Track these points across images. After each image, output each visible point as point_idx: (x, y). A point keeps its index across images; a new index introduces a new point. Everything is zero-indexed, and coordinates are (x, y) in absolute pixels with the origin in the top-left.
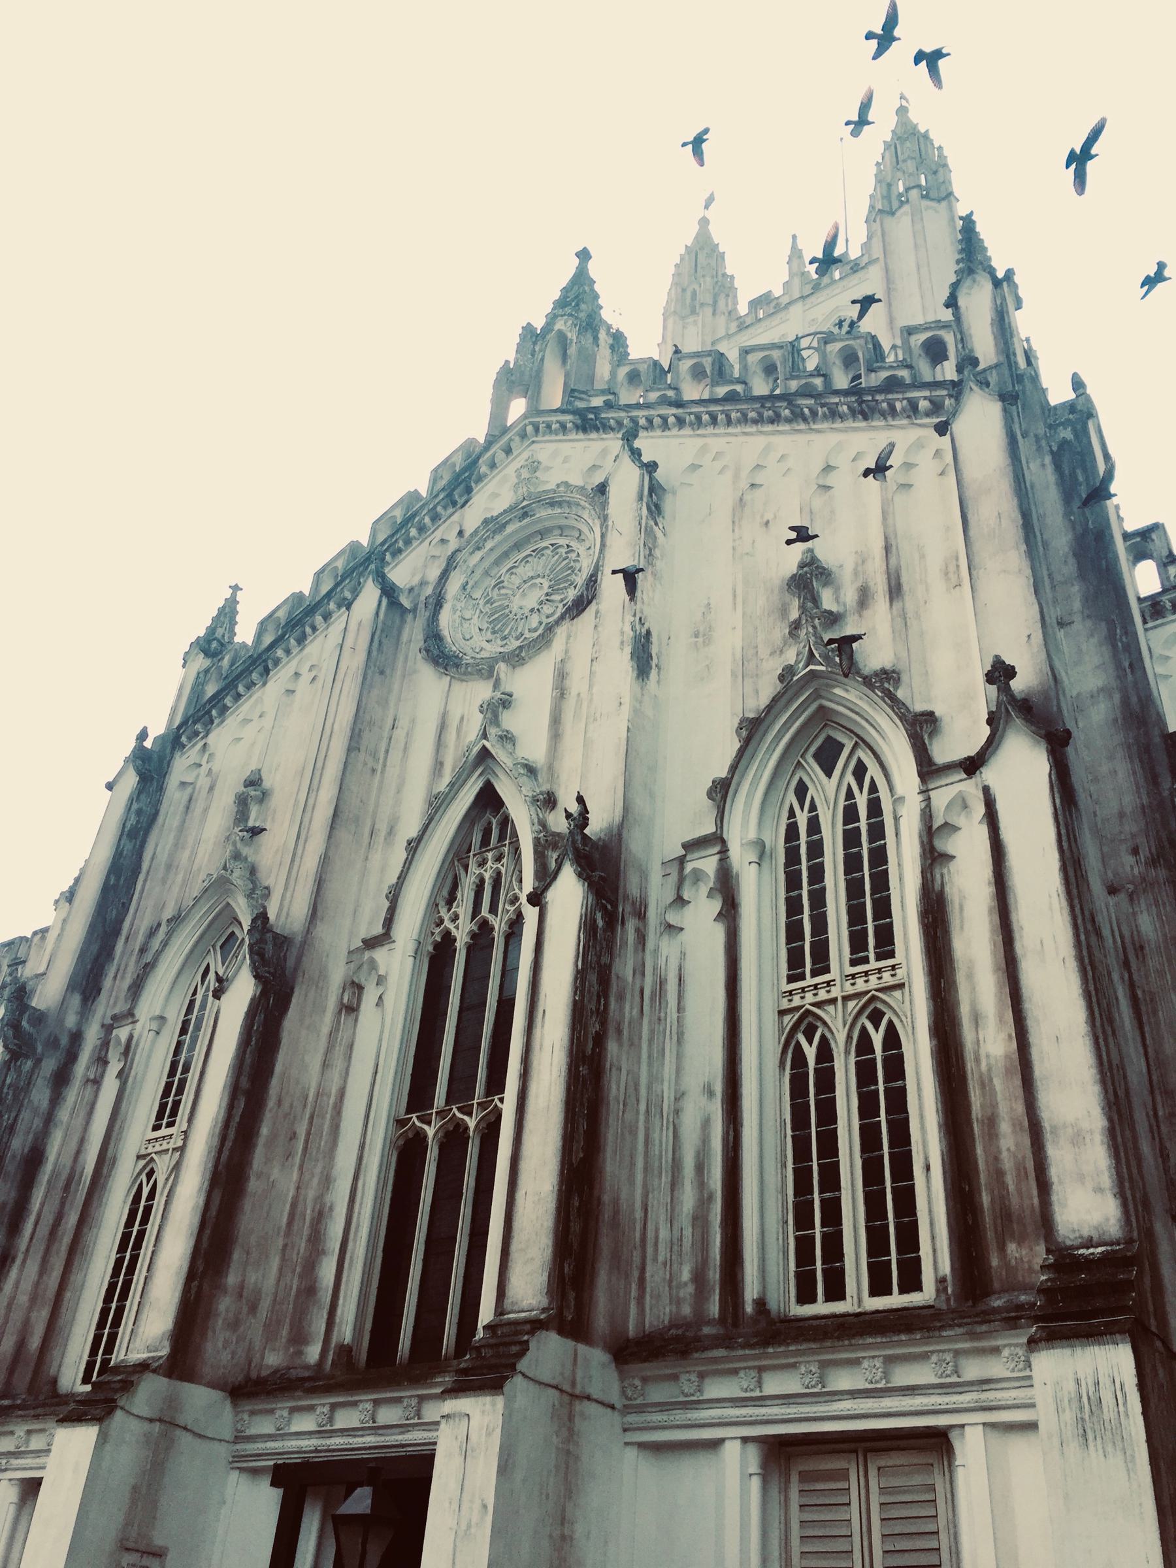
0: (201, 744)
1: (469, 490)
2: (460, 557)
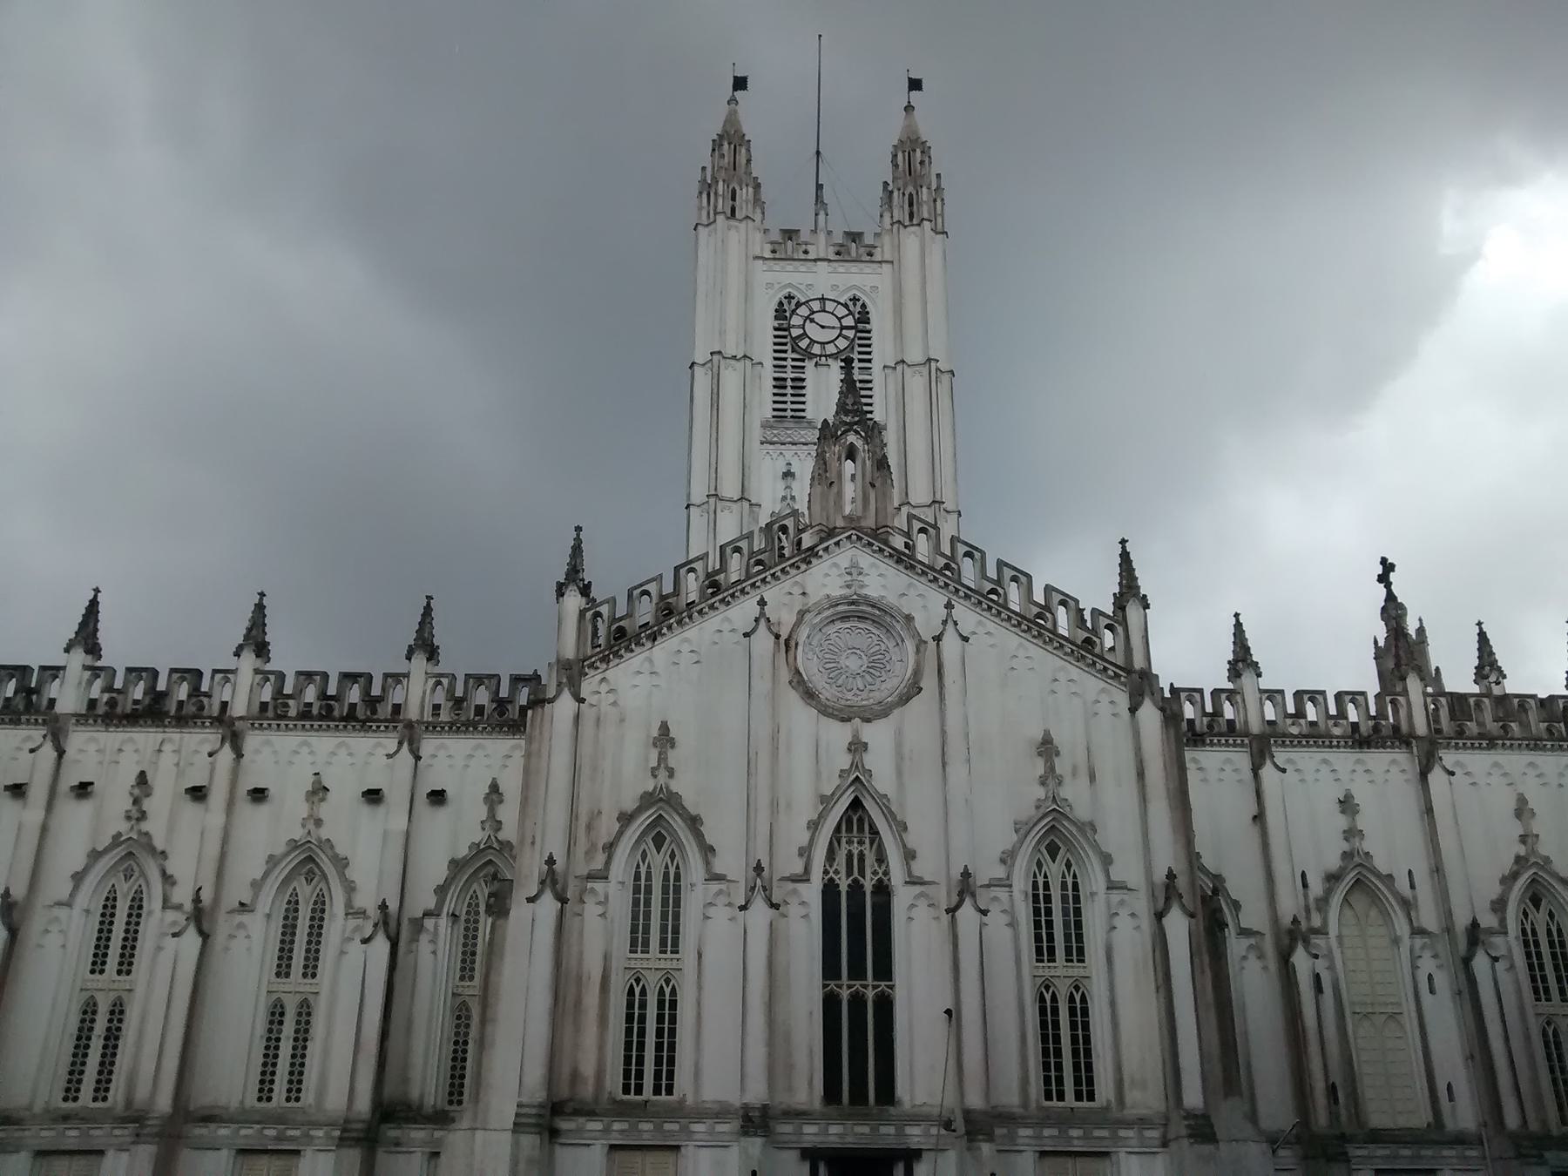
0: (599, 677)
2: (808, 617)
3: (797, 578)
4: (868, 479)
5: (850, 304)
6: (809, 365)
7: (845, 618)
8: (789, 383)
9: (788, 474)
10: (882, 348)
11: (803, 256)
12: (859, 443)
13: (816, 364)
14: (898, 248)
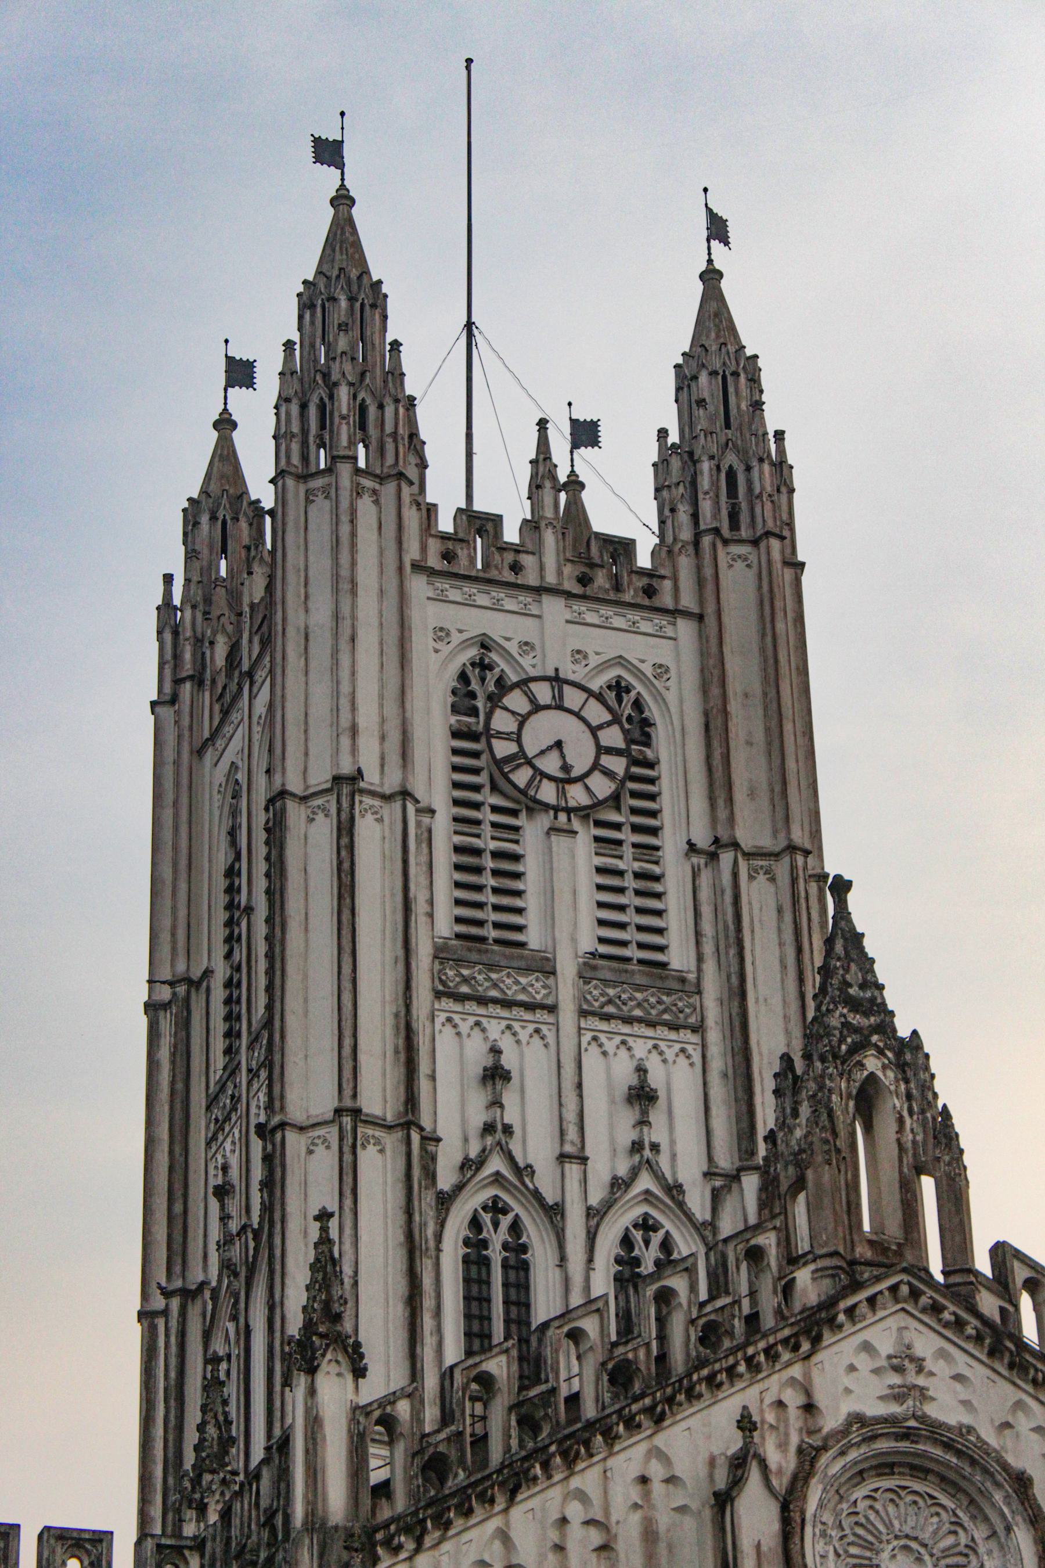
1: (816, 1341)
2: (824, 1459)
3: (796, 1371)
5: (611, 696)
6: (532, 831)
7: (885, 1467)
9: (495, 1075)
10: (682, 813)
11: (508, 576)
12: (888, 1078)
13: (553, 830)
14: (708, 583)
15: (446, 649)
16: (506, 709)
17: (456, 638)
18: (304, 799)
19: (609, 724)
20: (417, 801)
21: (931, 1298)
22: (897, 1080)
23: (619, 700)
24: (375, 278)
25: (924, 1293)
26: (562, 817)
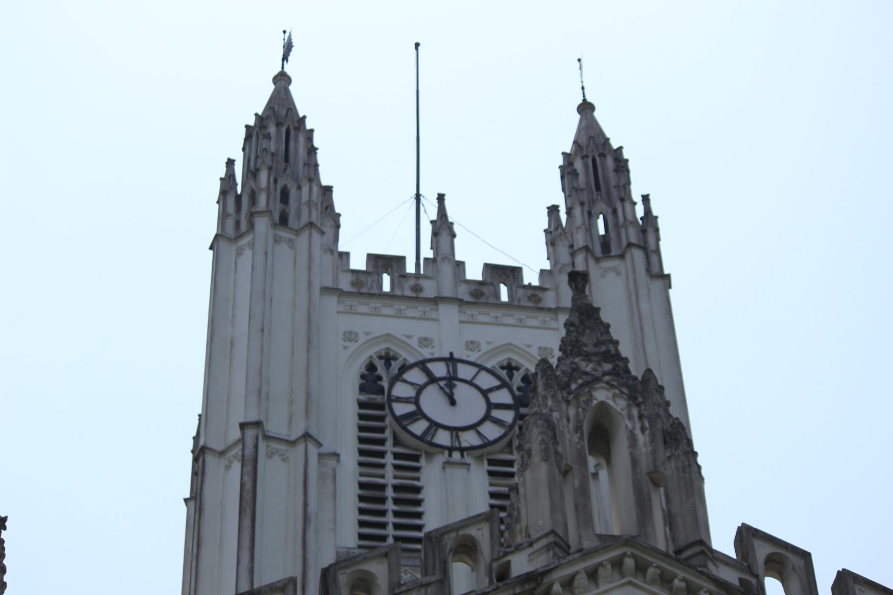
4: (645, 465)
5: (504, 373)
8: (390, 493)
13: (447, 463)
15: (353, 346)
16: (405, 381)
17: (363, 339)
18: (222, 453)
19: (498, 388)
20: (319, 445)
21: (658, 567)
22: (629, 406)
23: (511, 376)
24: (301, 115)
25: (651, 564)
26: (456, 455)
